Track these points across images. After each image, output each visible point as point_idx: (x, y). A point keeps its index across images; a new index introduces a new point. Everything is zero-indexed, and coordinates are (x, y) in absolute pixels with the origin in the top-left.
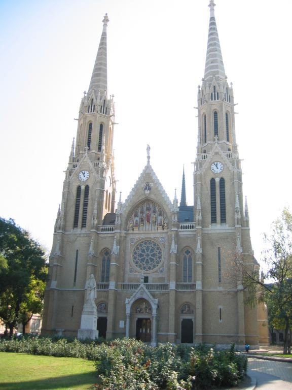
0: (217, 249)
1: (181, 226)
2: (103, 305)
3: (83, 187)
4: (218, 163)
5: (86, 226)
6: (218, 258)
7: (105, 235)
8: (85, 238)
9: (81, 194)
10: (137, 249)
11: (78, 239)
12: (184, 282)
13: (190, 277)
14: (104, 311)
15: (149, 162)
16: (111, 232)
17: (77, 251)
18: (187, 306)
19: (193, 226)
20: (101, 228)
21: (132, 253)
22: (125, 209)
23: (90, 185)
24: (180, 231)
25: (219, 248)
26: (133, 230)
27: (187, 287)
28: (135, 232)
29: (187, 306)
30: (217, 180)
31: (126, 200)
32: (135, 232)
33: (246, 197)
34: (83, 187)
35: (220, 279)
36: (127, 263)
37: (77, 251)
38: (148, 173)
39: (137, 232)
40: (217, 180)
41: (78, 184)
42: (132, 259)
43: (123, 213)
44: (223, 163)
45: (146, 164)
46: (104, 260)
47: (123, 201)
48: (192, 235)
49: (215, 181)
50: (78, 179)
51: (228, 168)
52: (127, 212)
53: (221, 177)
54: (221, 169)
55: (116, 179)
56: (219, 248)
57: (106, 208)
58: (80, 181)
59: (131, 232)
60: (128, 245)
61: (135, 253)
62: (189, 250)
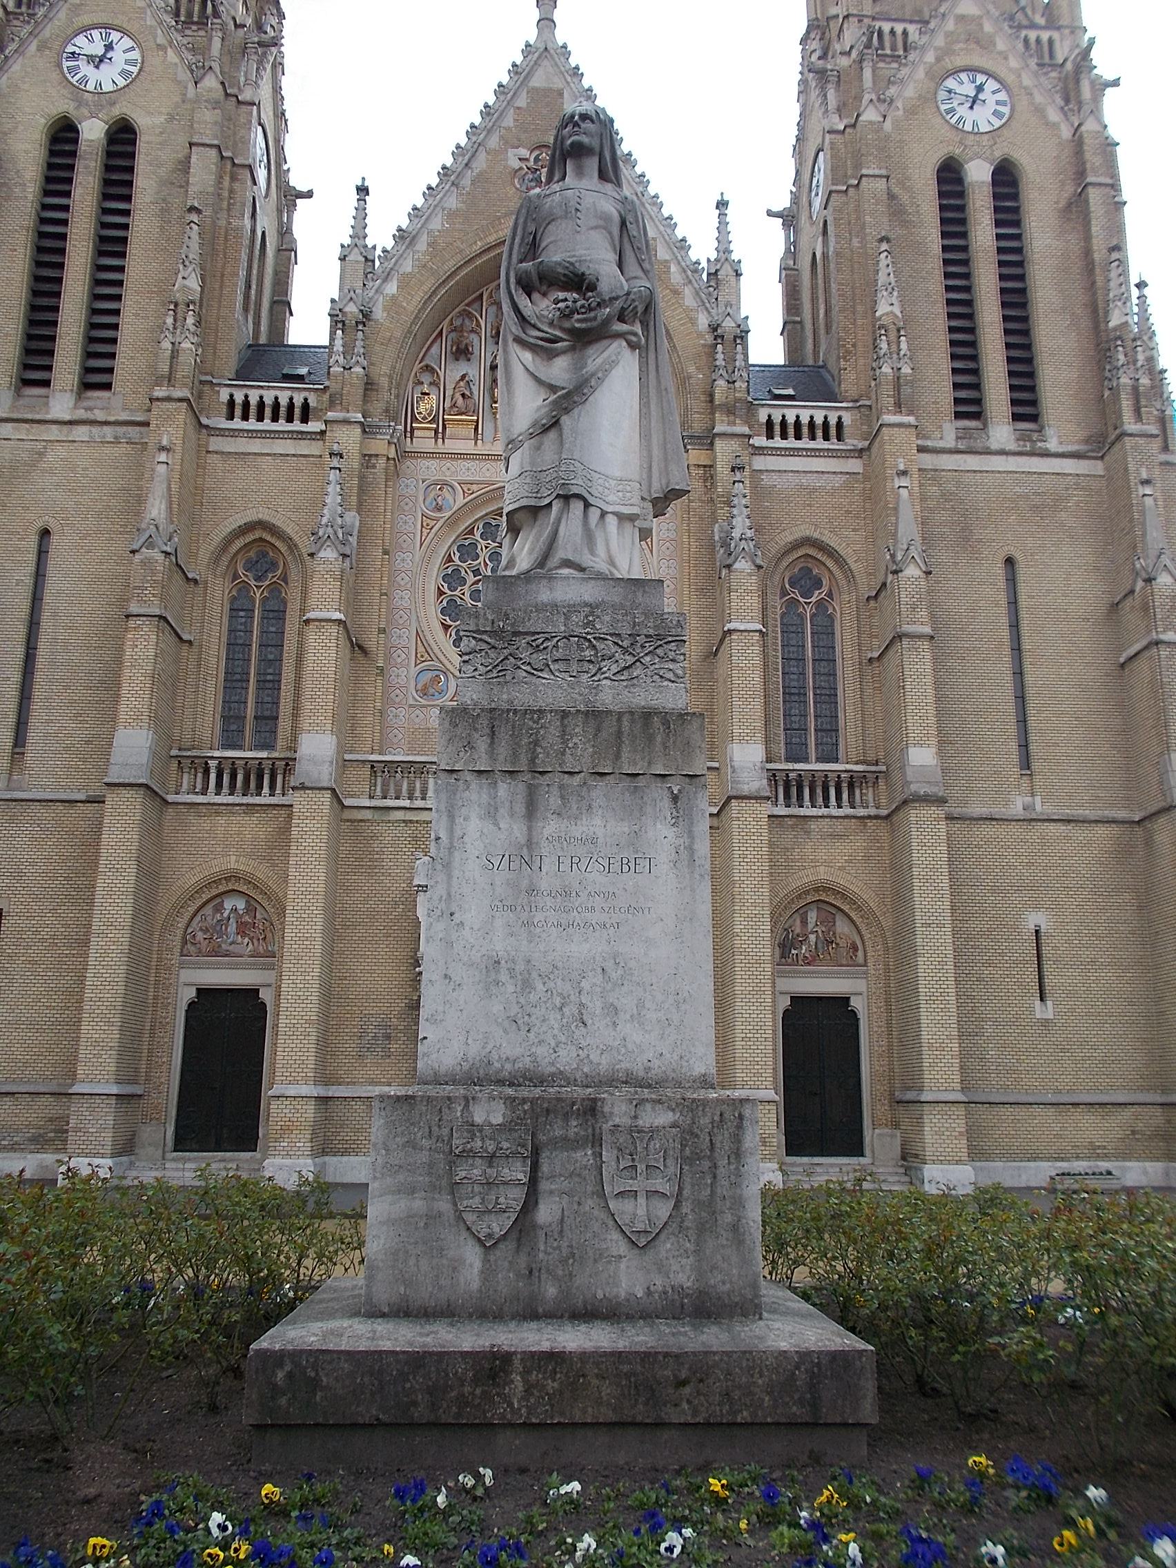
0: (999, 570)
1: (763, 418)
2: (228, 904)
3: (93, 131)
4: (991, 85)
5: (117, 379)
6: (1004, 621)
7: (256, 446)
8: (108, 450)
9: (80, 166)
10: (468, 551)
11: (56, 455)
12: (789, 759)
13: (830, 730)
14: (245, 945)
15: (546, 22)
16: (297, 426)
17: (45, 533)
18: (812, 916)
19: (840, 424)
20: (224, 395)
21: (433, 580)
22: (392, 288)
23: (142, 121)
24: (759, 451)
25: (1010, 562)
26: (439, 434)
27: (822, 788)
28: (451, 446)
29: (812, 916)
30: (979, 173)
31: (401, 236)
32: (451, 446)
33: (1141, 285)
34: (93, 131)
35: (1024, 746)
36: (404, 638)
37: (45, 533)
38: (547, 92)
39: (467, 446)
40: (979, 173)
41: (62, 105)
42: (432, 615)
43: (379, 313)
44: (1010, 79)
45: (531, 34)
46: (239, 609)
47: (381, 237)
48: (838, 481)
49: (960, 181)
50: (55, 76)
51: (1039, 111)
52: (412, 304)
53: (998, 154)
54: (996, 113)
55: (298, 181)
56: (1010, 562)
57: (246, 309)
58: (77, 91)
59: (424, 441)
60: (412, 524)
61: (454, 579)
62: (815, 571)
